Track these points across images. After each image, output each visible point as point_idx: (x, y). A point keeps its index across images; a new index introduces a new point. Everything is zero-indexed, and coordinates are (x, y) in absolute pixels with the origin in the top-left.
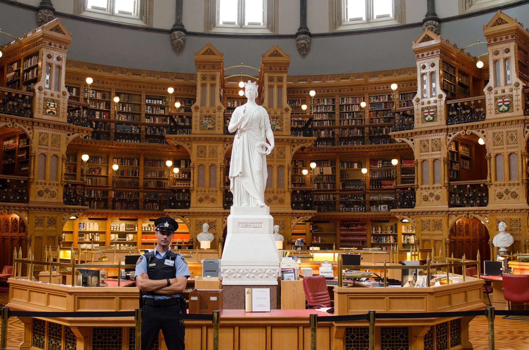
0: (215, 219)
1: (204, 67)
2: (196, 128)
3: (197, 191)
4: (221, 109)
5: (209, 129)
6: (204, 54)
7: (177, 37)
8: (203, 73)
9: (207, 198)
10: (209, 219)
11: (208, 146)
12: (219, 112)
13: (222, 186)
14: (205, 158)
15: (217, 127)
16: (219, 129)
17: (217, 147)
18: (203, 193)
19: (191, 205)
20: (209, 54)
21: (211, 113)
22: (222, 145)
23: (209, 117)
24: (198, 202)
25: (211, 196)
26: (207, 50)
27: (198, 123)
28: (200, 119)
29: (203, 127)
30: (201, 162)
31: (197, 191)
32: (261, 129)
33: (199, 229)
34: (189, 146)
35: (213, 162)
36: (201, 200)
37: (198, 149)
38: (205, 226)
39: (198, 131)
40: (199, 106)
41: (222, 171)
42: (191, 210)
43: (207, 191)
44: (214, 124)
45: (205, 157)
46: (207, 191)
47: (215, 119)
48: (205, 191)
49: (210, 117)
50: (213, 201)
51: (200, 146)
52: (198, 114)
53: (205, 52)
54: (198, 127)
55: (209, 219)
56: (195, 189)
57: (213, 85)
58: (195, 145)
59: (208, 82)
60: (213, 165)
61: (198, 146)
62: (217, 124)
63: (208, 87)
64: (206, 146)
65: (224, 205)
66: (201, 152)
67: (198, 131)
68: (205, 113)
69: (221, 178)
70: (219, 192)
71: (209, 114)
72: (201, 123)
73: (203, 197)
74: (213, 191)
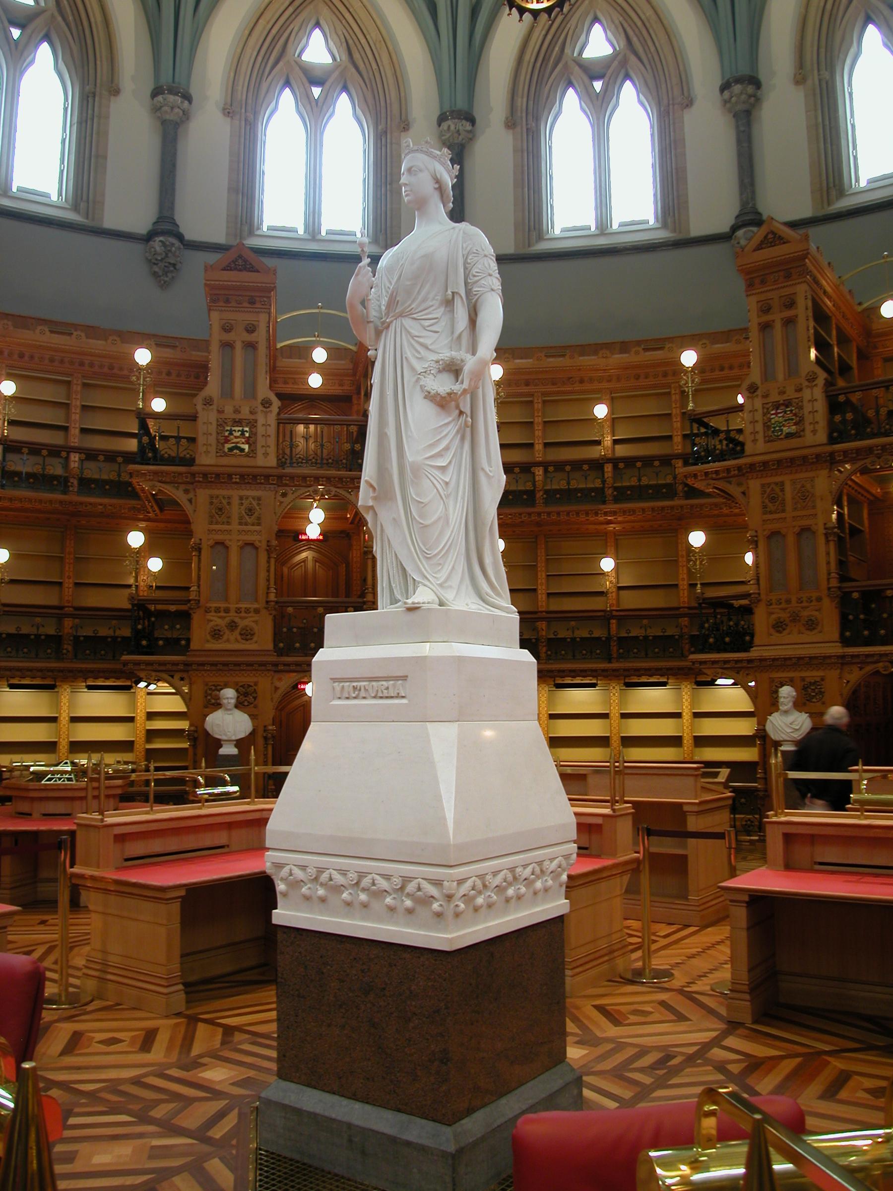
0: (820, 673)
1: (763, 282)
2: (755, 441)
3: (769, 603)
4: (814, 379)
5: (789, 436)
6: (759, 247)
7: (743, 242)
8: (763, 297)
9: (795, 618)
10: (804, 674)
11: (789, 482)
12: (812, 387)
13: (834, 583)
14: (783, 515)
15: (809, 428)
16: (814, 432)
17: (812, 479)
18: (783, 605)
19: (757, 641)
20: (772, 244)
21: (791, 394)
22: (824, 473)
23: (787, 406)
24: (772, 631)
25: (805, 613)
26: (766, 237)
27: (759, 427)
28: (764, 415)
29: (771, 434)
30: (775, 526)
31: (769, 603)
32: (449, 303)
33: (773, 705)
34: (741, 489)
35: (805, 522)
36: (779, 626)
37: (763, 493)
38: (786, 692)
39: (761, 446)
40: (759, 383)
41: (832, 544)
42: (754, 653)
43: (794, 600)
44: (800, 422)
45: (783, 511)
46: (794, 600)
47: (801, 408)
48: (788, 601)
49: (787, 403)
50: (811, 625)
51: (769, 484)
52: (758, 403)
53: (762, 242)
54: (760, 437)
55: (804, 674)
56: (763, 596)
57: (789, 322)
58: (754, 485)
59: (777, 317)
60: (805, 530)
61: (763, 485)
62: (808, 419)
63: (778, 330)
64: (782, 484)
65: (842, 635)
66: (773, 499)
67: (761, 446)
68: (775, 397)
69: (828, 563)
70: (826, 602)
71: (785, 397)
72: (767, 426)
73: (784, 615)
74: (810, 600)
